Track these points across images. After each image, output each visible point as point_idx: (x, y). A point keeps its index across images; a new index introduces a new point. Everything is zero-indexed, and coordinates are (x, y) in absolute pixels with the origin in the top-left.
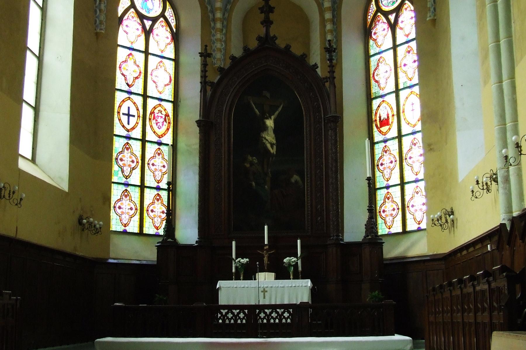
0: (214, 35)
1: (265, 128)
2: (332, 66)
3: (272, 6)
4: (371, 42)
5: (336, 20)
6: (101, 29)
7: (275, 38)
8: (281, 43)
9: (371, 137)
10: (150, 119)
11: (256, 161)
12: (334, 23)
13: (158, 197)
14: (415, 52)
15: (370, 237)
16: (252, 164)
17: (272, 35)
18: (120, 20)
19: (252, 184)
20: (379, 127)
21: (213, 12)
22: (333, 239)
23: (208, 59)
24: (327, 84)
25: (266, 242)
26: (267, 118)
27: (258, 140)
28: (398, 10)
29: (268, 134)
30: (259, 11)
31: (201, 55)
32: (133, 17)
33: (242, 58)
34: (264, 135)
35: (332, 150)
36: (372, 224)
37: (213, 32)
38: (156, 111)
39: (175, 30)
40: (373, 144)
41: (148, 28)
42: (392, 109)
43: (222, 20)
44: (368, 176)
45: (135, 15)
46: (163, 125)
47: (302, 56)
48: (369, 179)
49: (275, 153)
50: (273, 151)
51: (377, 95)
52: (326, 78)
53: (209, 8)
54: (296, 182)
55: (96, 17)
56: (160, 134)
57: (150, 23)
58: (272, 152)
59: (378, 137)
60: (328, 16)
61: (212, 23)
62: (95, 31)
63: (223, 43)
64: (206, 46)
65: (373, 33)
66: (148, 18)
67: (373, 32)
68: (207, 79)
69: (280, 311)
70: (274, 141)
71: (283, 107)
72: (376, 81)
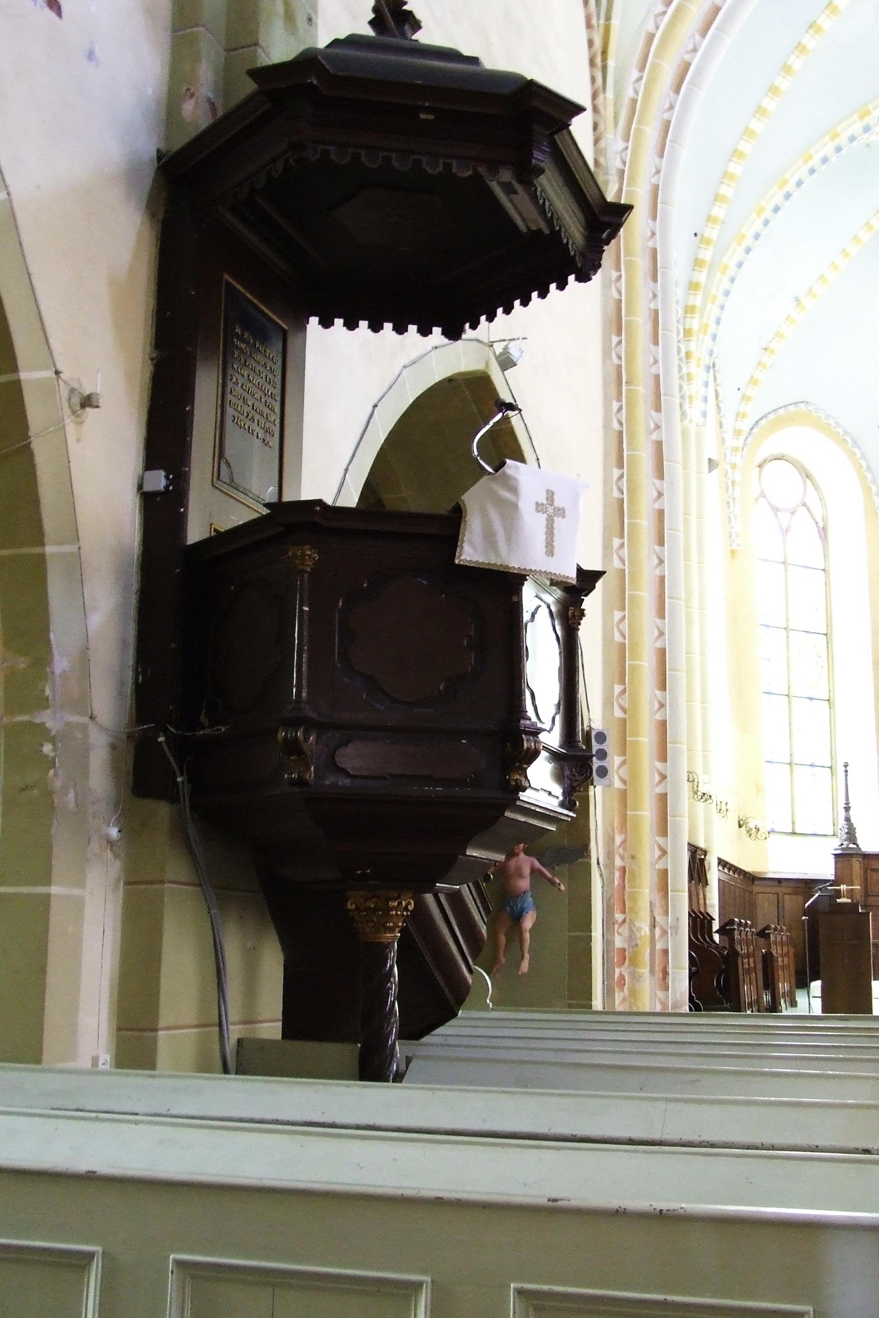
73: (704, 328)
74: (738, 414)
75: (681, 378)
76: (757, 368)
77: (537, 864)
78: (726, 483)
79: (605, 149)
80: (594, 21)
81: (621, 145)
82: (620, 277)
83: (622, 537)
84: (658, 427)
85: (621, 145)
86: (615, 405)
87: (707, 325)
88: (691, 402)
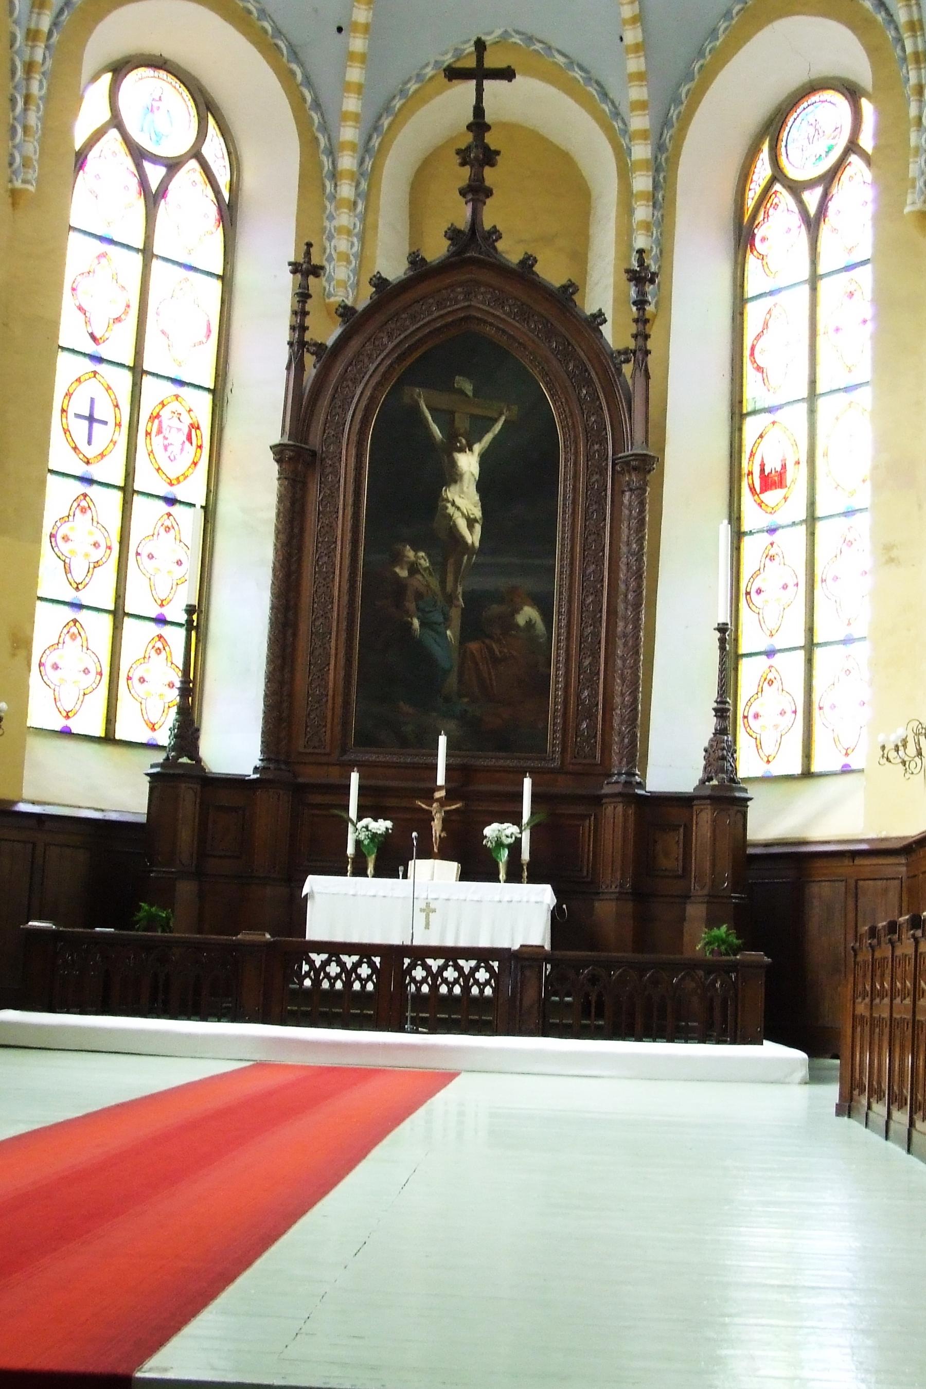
0: (331, 218)
1: (453, 476)
2: (642, 321)
4: (752, 262)
6: (25, 181)
7: (495, 233)
9: (735, 518)
10: (148, 434)
11: (425, 563)
13: (159, 645)
14: (868, 295)
15: (715, 782)
16: (414, 569)
17: (487, 226)
18: (80, 159)
19: (412, 624)
20: (758, 490)
21: (331, 152)
22: (617, 782)
23: (311, 278)
24: (627, 369)
25: (441, 780)
26: (461, 450)
28: (830, 178)
29: (462, 492)
30: (457, 160)
31: (296, 268)
32: (114, 154)
33: (404, 286)
34: (451, 493)
35: (628, 544)
36: (723, 749)
37: (330, 207)
38: (165, 413)
40: (738, 535)
41: (154, 186)
43: (357, 178)
44: (721, 621)
45: (122, 149)
46: (182, 450)
47: (565, 288)
48: (722, 629)
49: (477, 544)
50: (473, 537)
52: (626, 351)
54: (530, 624)
55: (14, 147)
56: (173, 476)
58: (470, 541)
59: (751, 517)
60: (642, 182)
61: (328, 183)
62: (10, 186)
63: (355, 240)
64: (309, 245)
66: (156, 159)
67: (759, 233)
68: (308, 337)
69: (467, 965)
70: (477, 513)
72: (759, 369)
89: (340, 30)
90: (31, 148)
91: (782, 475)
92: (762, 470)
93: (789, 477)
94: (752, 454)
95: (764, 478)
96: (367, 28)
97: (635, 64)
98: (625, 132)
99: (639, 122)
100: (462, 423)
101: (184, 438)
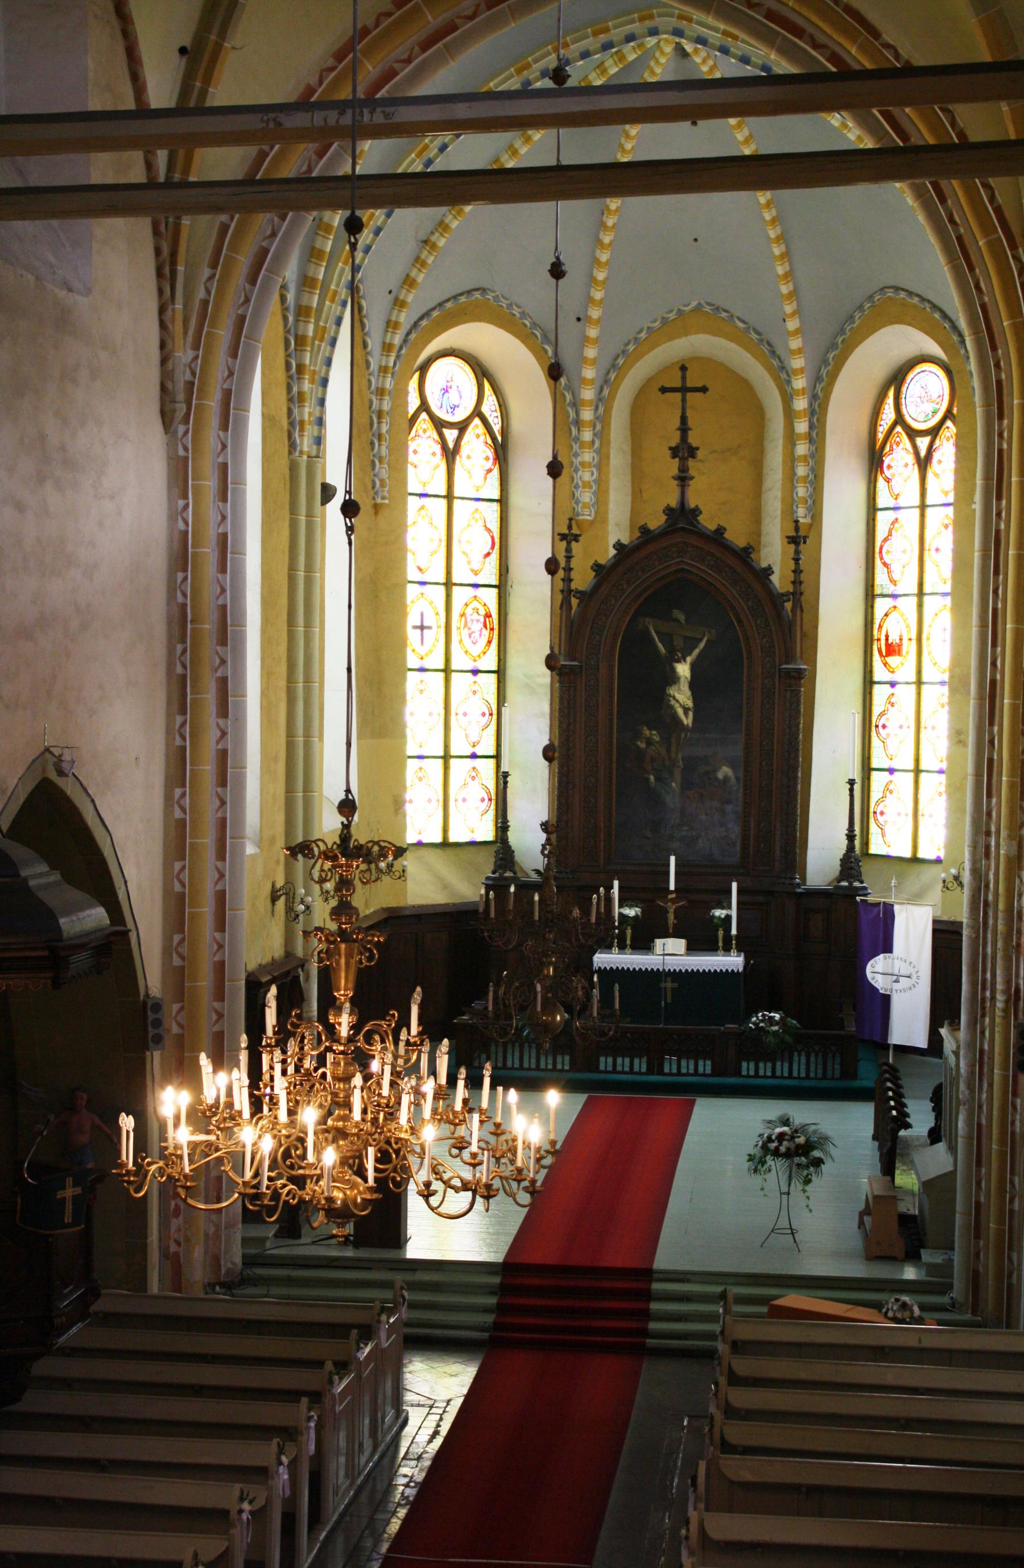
0: (576, 455)
1: (673, 678)
2: (797, 560)
3: (694, 445)
4: (881, 483)
5: (817, 436)
6: (383, 498)
8: (708, 522)
10: (458, 628)
11: (657, 738)
12: (811, 441)
15: (845, 884)
16: (649, 742)
17: (692, 506)
19: (648, 779)
21: (576, 404)
23: (574, 544)
24: (788, 606)
25: (672, 887)
26: (679, 661)
27: (660, 700)
28: (934, 432)
29: (680, 689)
32: (425, 431)
34: (672, 691)
37: (576, 447)
38: (469, 611)
39: (500, 438)
41: (451, 445)
42: (908, 626)
49: (690, 725)
50: (688, 721)
51: (885, 592)
52: (787, 594)
53: (569, 397)
54: (726, 779)
57: (455, 433)
58: (685, 722)
59: (879, 673)
60: (802, 427)
61: (573, 429)
63: (594, 470)
65: (885, 465)
66: (451, 425)
67: (887, 461)
68: (573, 586)
70: (690, 704)
71: (708, 641)
73: (320, 333)
74: (388, 323)
75: (290, 400)
76: (413, 265)
77: (97, 1120)
78: (371, 417)
79: (173, 370)
80: (163, 228)
81: (191, 354)
82: (186, 506)
83: (184, 785)
84: (223, 662)
85: (191, 354)
86: (179, 648)
87: (325, 328)
88: (302, 430)
89: (579, 319)
90: (384, 474)
91: (900, 646)
92: (887, 639)
93: (904, 649)
94: (880, 627)
95: (888, 646)
96: (598, 321)
97: (795, 343)
98: (789, 382)
99: (799, 383)
100: (678, 642)
101: (482, 625)
